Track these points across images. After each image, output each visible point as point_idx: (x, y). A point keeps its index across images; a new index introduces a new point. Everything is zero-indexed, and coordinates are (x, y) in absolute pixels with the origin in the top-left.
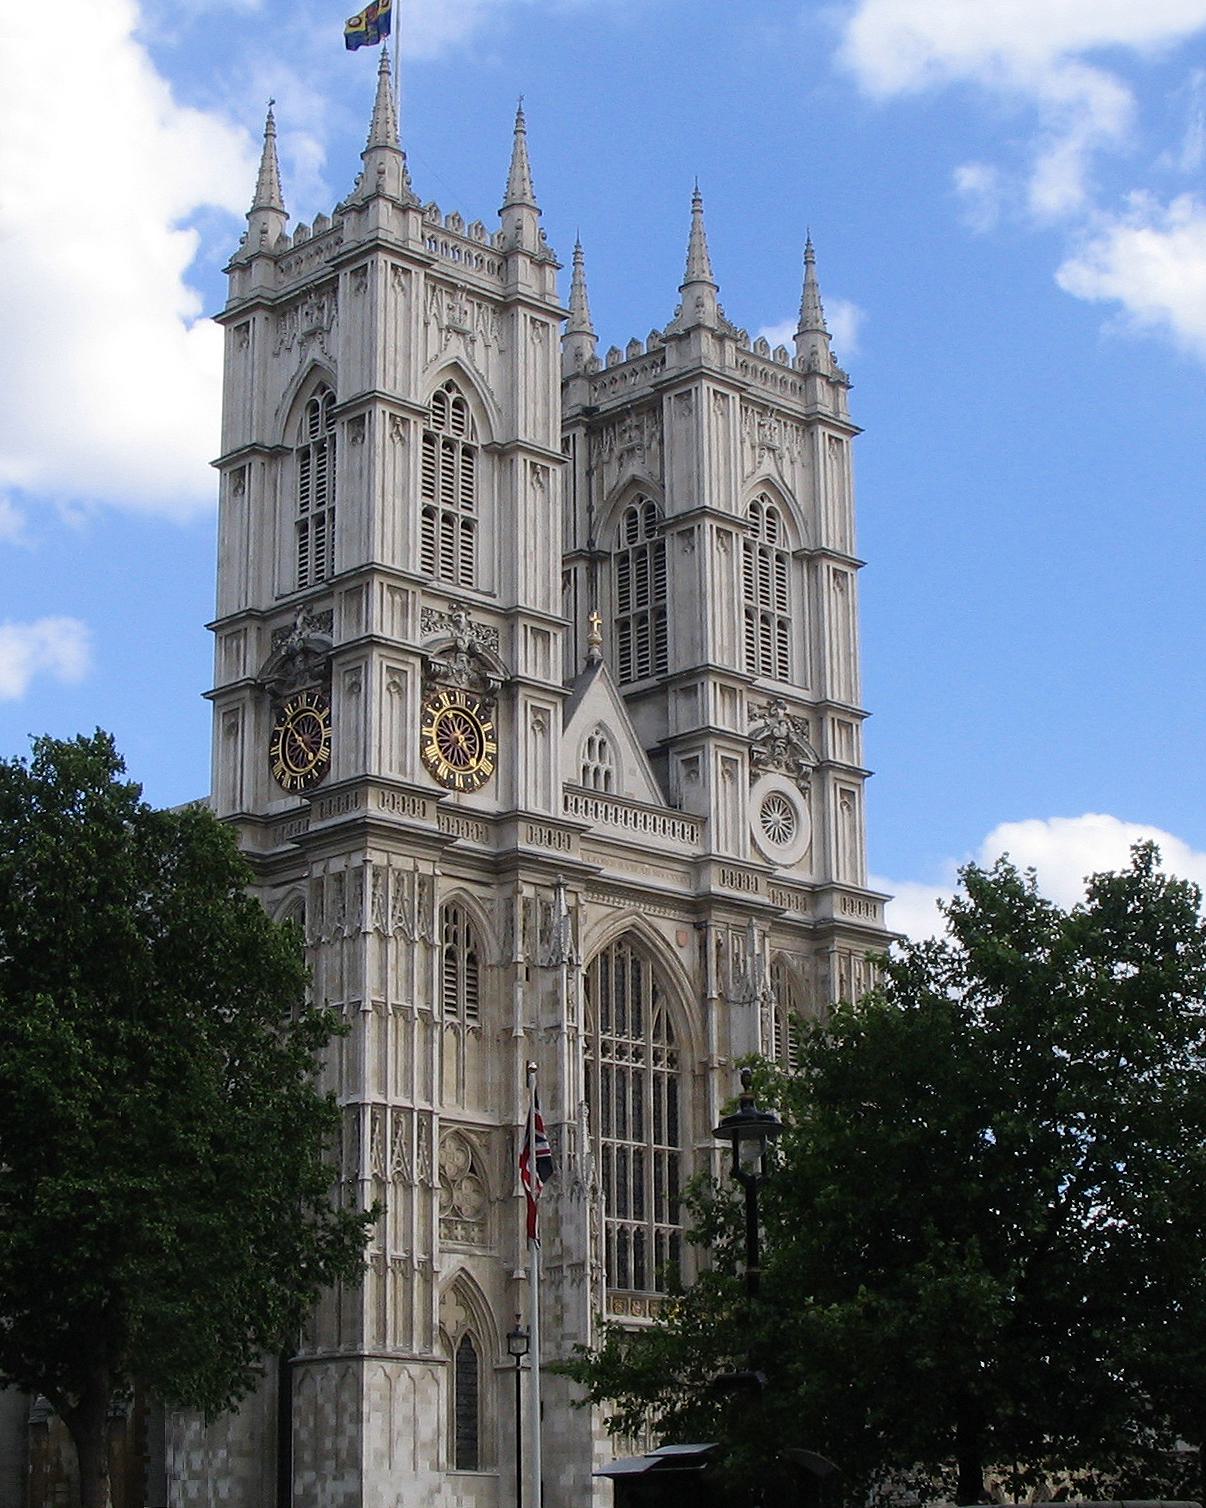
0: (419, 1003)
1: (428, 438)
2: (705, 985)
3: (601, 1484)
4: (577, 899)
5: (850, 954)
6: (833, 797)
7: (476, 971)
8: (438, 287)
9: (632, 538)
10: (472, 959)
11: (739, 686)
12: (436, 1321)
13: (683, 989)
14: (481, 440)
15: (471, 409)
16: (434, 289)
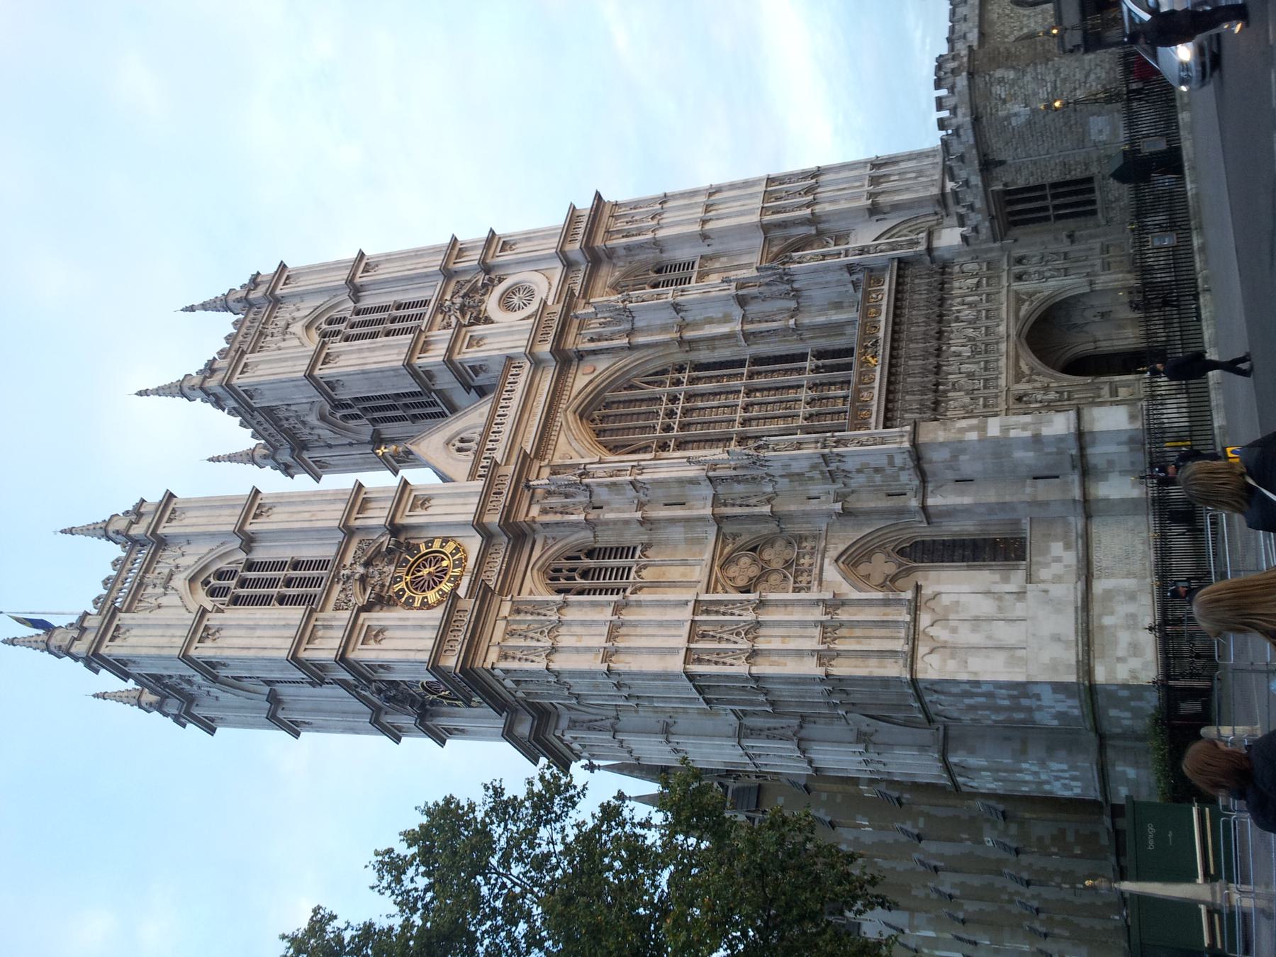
0: (607, 615)
1: (236, 601)
2: (622, 348)
3: (1032, 426)
4: (545, 466)
5: (609, 232)
6: (507, 257)
7: (600, 549)
8: (139, 597)
9: (359, 417)
10: (590, 554)
11: (423, 339)
12: (879, 595)
13: (625, 366)
14: (242, 556)
15: (222, 565)
16: (140, 601)
